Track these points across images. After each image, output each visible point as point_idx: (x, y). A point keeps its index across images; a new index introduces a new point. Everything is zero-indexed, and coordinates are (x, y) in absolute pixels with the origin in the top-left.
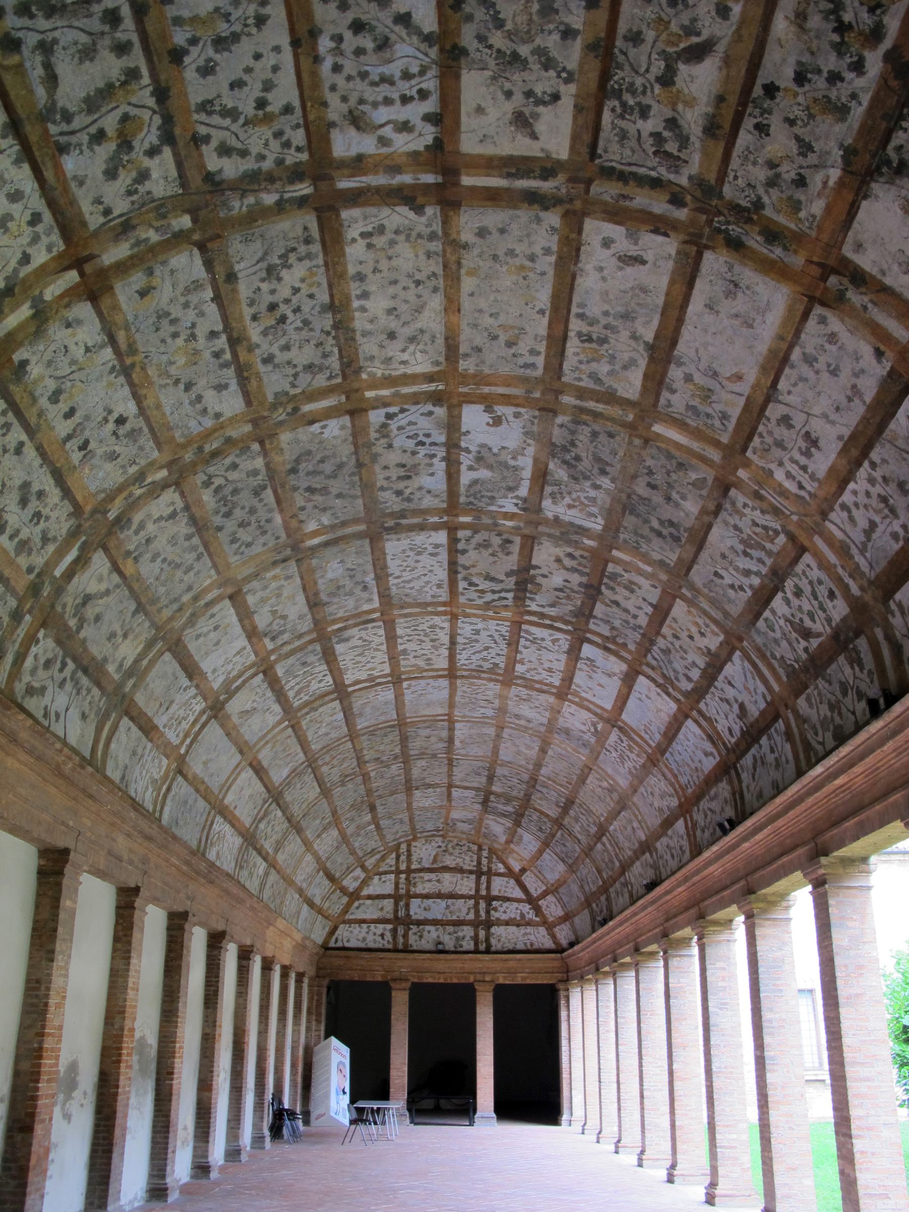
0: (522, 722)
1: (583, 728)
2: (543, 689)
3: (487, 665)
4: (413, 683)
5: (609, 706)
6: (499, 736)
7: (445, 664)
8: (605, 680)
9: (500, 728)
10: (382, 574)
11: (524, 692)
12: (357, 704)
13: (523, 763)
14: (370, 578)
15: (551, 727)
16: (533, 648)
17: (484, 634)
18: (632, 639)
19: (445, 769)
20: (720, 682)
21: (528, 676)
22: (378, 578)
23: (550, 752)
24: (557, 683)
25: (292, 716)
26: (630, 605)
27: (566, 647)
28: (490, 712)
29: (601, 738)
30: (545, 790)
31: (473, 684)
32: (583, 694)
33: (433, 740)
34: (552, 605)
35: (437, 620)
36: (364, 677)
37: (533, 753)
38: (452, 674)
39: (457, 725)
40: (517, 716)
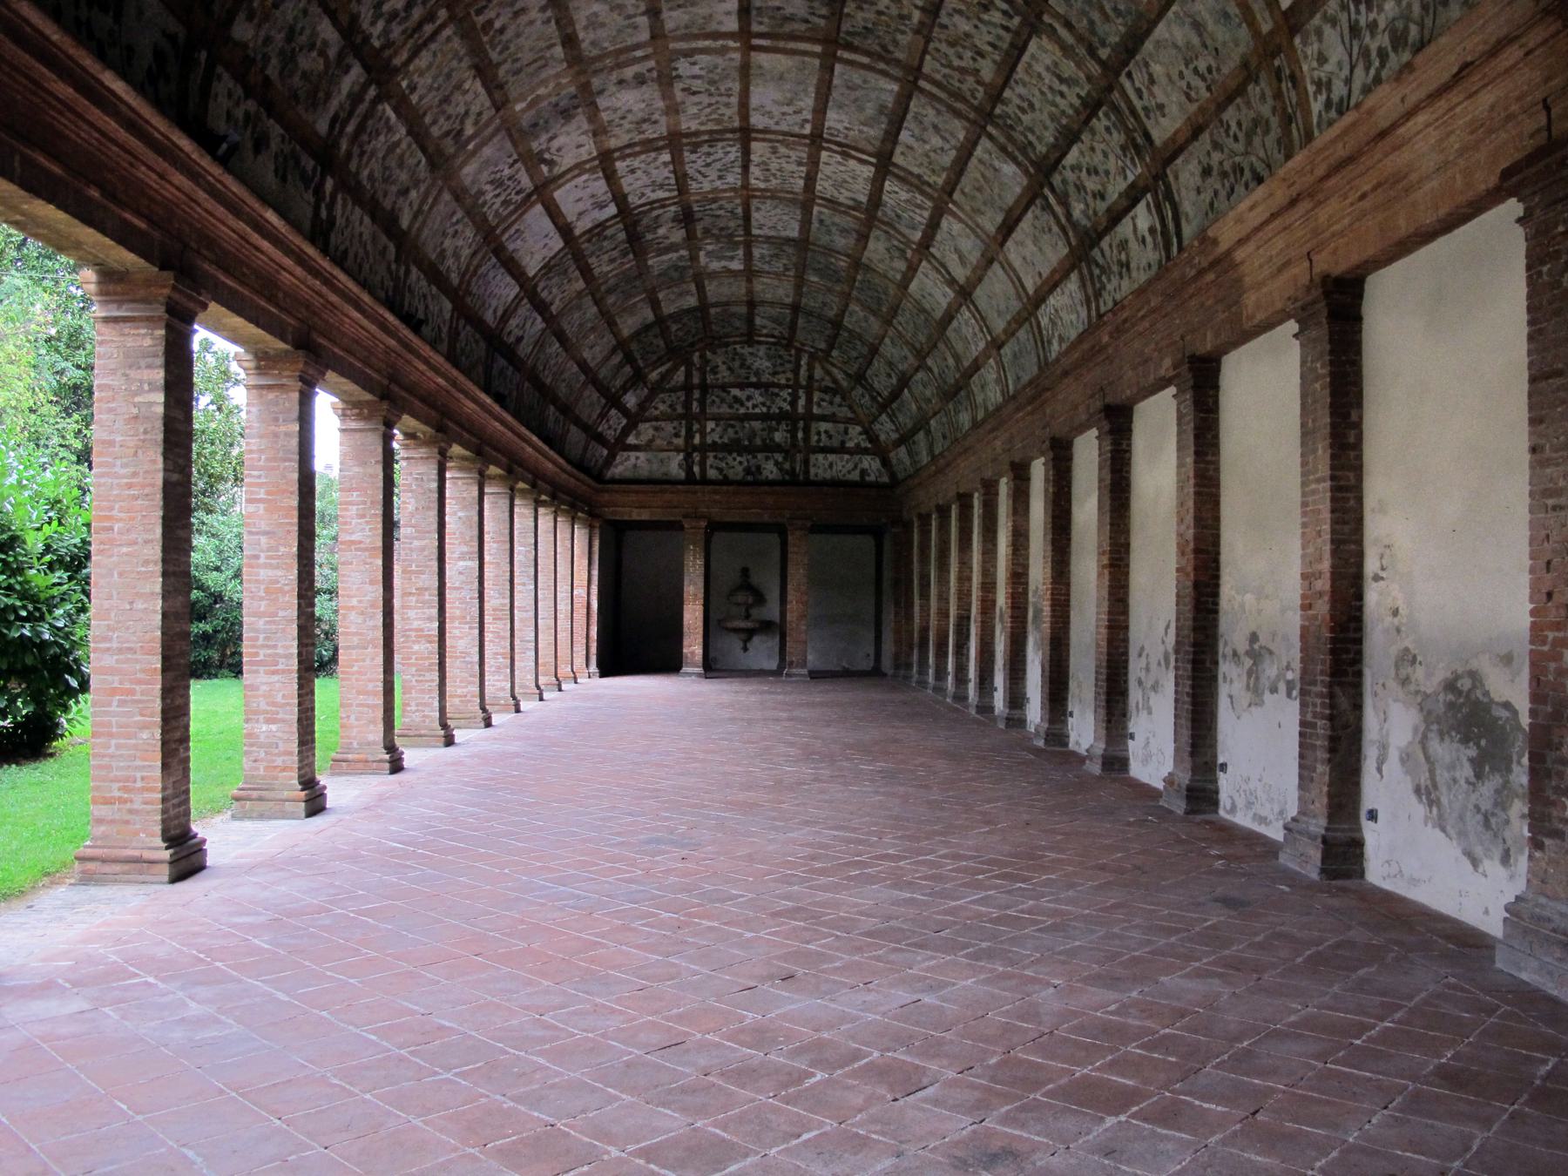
0: (629, 72)
1: (555, 144)
2: (627, 151)
3: (705, 149)
4: (796, 130)
5: (557, 195)
7: (754, 145)
8: (581, 206)
9: (657, 35)
10: (806, 224)
11: (650, 133)
12: (875, 132)
14: (815, 224)
15: (586, 99)
16: (659, 180)
17: (713, 174)
20: (535, 314)
21: (653, 155)
22: (810, 223)
23: (558, 51)
24: (618, 164)
26: (606, 257)
27: (630, 199)
28: (683, 67)
29: (532, 160)
31: (718, 122)
32: (585, 177)
34: (658, 217)
35: (762, 185)
36: (852, 163)
38: (746, 134)
39: (732, 25)
40: (640, 80)
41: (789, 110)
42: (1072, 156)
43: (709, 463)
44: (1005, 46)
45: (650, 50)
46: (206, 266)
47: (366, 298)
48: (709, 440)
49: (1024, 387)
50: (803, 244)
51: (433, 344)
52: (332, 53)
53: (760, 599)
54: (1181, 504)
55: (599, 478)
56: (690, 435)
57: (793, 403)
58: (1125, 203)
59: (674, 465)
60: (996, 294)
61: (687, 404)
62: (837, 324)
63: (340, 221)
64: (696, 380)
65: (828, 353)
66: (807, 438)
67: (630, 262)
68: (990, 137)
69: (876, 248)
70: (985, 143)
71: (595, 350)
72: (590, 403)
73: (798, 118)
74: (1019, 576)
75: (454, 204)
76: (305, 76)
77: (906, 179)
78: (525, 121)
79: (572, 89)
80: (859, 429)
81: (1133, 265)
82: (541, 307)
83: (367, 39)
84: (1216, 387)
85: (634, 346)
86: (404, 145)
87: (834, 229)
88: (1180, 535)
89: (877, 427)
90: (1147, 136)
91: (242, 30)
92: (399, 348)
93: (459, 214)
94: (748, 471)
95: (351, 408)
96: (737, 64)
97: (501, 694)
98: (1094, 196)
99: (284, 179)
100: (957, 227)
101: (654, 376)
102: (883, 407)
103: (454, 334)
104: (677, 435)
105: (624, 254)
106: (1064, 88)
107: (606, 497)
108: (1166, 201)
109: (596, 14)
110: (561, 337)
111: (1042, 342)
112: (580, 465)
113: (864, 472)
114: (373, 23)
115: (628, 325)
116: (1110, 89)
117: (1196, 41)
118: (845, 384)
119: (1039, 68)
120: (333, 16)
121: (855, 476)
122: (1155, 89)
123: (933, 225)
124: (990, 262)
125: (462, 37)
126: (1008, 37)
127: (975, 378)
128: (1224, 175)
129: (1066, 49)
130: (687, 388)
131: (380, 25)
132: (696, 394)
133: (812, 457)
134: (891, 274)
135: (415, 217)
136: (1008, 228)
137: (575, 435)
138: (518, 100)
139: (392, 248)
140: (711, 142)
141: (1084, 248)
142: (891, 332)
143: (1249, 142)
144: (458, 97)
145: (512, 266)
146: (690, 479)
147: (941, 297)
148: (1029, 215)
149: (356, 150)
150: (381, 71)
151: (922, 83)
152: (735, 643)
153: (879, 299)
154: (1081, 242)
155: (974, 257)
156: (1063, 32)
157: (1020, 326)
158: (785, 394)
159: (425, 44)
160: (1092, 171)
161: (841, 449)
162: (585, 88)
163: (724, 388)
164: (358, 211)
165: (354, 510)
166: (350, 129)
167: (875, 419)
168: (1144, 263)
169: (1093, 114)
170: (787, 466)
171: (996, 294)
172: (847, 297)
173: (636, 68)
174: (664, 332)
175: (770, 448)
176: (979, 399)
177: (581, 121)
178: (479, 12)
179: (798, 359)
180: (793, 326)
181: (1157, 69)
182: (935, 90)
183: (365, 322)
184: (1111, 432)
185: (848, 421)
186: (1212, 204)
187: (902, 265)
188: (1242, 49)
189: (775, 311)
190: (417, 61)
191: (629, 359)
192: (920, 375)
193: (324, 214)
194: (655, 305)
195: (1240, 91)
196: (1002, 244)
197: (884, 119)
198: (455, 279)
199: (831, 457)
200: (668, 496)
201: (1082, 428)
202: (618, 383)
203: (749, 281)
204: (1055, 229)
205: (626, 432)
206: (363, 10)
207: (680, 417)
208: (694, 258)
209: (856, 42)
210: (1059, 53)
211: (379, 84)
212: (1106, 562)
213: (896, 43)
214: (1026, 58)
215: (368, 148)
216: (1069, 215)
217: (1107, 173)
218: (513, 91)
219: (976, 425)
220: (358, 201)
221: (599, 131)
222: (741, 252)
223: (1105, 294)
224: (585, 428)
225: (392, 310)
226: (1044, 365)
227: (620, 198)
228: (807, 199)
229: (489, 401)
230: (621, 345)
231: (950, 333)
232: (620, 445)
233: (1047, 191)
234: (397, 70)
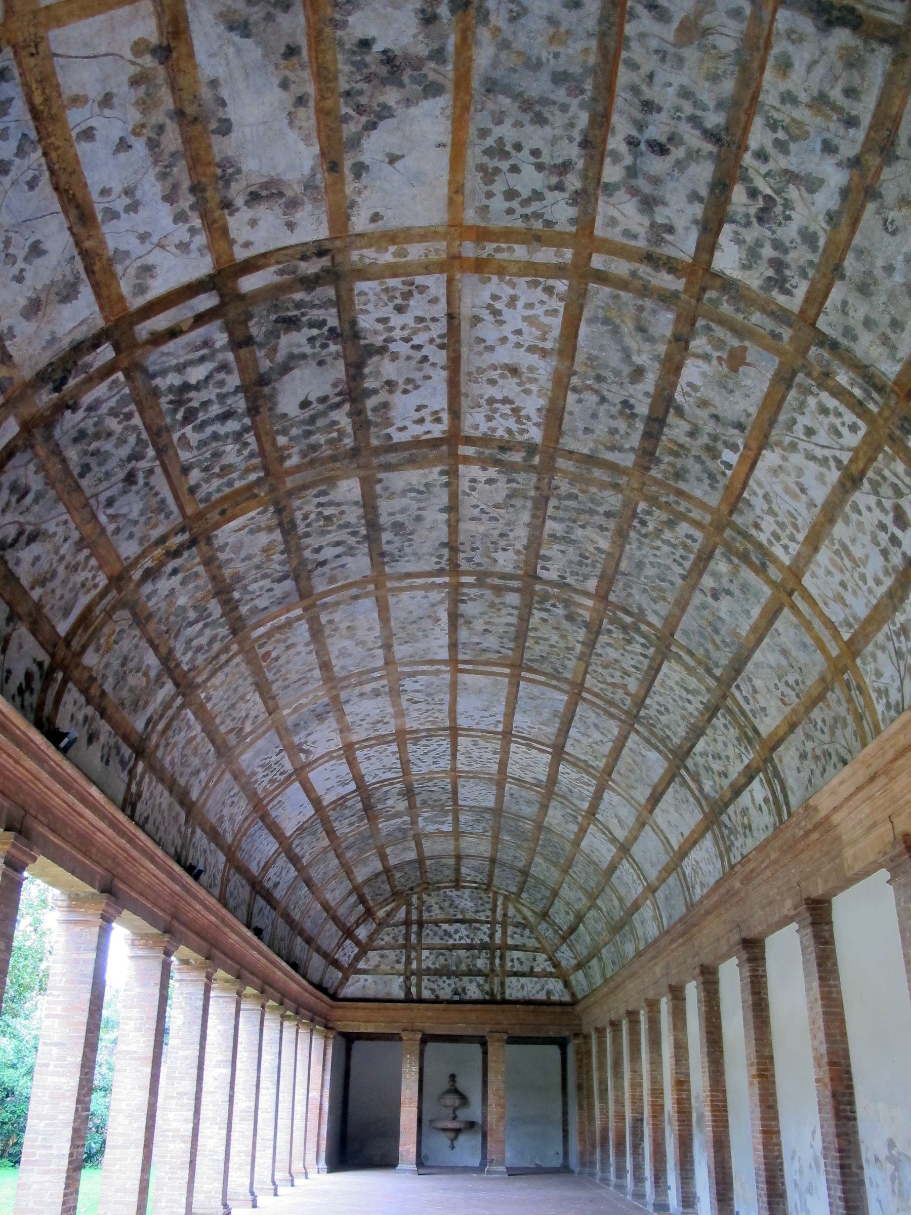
0: (368, 688)
1: (311, 739)
3: (424, 742)
4: (491, 728)
5: (310, 775)
6: (387, 647)
8: (328, 784)
9: (389, 662)
10: (500, 797)
11: (383, 730)
12: (551, 730)
13: (337, 617)
14: (507, 798)
15: (336, 706)
17: (429, 760)
18: (332, 815)
19: (466, 527)
20: (290, 865)
23: (317, 673)
25: (604, 779)
28: (408, 684)
29: (293, 750)
30: (280, 589)
31: (433, 722)
33: (479, 625)
36: (534, 752)
37: (336, 645)
38: (454, 732)
39: (444, 654)
40: (376, 693)
41: (487, 714)
42: (700, 746)
43: (424, 984)
44: (645, 668)
45: (384, 672)
46: (41, 829)
47: (159, 852)
48: (424, 966)
49: (675, 924)
50: (497, 811)
51: (208, 889)
52: (153, 674)
53: (464, 1100)
54: (813, 1022)
55: (334, 997)
56: (408, 962)
57: (492, 936)
58: (743, 780)
59: (396, 988)
60: (650, 850)
61: (407, 937)
62: (525, 873)
63: (145, 794)
64: (414, 917)
65: (518, 895)
66: (502, 965)
67: (364, 825)
68: (637, 732)
69: (555, 816)
70: (633, 736)
71: (336, 892)
72: (329, 936)
73: (494, 720)
74: (682, 1084)
75: (233, 782)
76: (131, 690)
77: (575, 763)
78: (290, 722)
79: (326, 700)
80: (545, 956)
81: (754, 827)
82: (294, 859)
83: (178, 665)
84: (830, 923)
85: (366, 890)
86: (199, 739)
87: (521, 801)
88: (815, 1050)
89: (558, 955)
90: (756, 731)
91: (90, 659)
92: (183, 893)
93: (237, 789)
94: (456, 993)
95: (140, 938)
96: (448, 681)
97: (241, 1190)
98: (720, 775)
99: (107, 763)
100: (616, 799)
101: (381, 913)
102: (564, 939)
103: (226, 881)
104: (398, 962)
105: (361, 819)
106: (690, 697)
107: (338, 1013)
108: (775, 779)
109: (345, 648)
110: (309, 883)
111: (687, 887)
112: (319, 987)
113: (549, 993)
114: (184, 654)
115: (361, 874)
116: (724, 697)
117: (784, 662)
118: (532, 919)
119: (671, 683)
120: (155, 648)
121: (542, 996)
122: (758, 696)
123: (598, 797)
124: (643, 825)
125: (248, 663)
126: (646, 662)
127: (636, 916)
128: (817, 758)
129: (690, 670)
130: (407, 923)
131: (189, 655)
132: (415, 928)
133: (508, 980)
134: (566, 834)
135: (203, 792)
136: (655, 799)
137: (317, 963)
138: (285, 707)
139: (183, 816)
140: (428, 737)
141: (714, 814)
142: (567, 879)
143: (833, 734)
144: (241, 705)
145: (274, 829)
146: (408, 1000)
147: (606, 852)
148: (671, 790)
149: (163, 742)
150: (185, 686)
151: (584, 694)
152: (443, 1140)
153: (557, 854)
154: (712, 809)
155: (631, 821)
156: (686, 658)
157: (670, 874)
158: (485, 928)
159: (221, 668)
160: (717, 757)
161: (531, 973)
162: (335, 699)
163: (436, 923)
164: (160, 787)
165: (132, 1024)
166: (160, 727)
167: (557, 949)
168: (762, 826)
169: (713, 715)
170: (487, 988)
171: (650, 850)
172: (533, 852)
173: (374, 685)
174: (390, 879)
175: (472, 973)
176: (640, 933)
177: (331, 722)
178: (261, 646)
179: (495, 901)
180: (491, 876)
181: (758, 683)
182: (594, 699)
183: (157, 872)
184: (749, 960)
185: (536, 950)
186: (810, 781)
187: (575, 828)
188: (819, 668)
189: (476, 863)
190: (213, 680)
191: (362, 900)
192: (592, 913)
193: (134, 788)
194: (383, 857)
195: (821, 697)
196: (651, 812)
197: (557, 720)
198: (229, 838)
199: (523, 980)
200: (391, 1013)
201: (725, 957)
202: (353, 919)
203: (457, 839)
204: (691, 800)
205: (357, 959)
206: (178, 645)
207: (404, 946)
208: (414, 822)
209: (535, 666)
210: (685, 673)
211: (184, 695)
212: (755, 1072)
213: (564, 667)
214: (660, 676)
215: (172, 741)
216: (701, 790)
217: (728, 758)
218: (282, 702)
219: (639, 954)
220: (161, 780)
221: (344, 729)
222: (450, 818)
223: (734, 849)
224: (325, 955)
225: (179, 862)
226: (691, 906)
227: (358, 778)
228: (501, 780)
229: (249, 934)
230: (356, 889)
231: (614, 879)
232: (352, 969)
233: (683, 772)
234: (198, 686)
